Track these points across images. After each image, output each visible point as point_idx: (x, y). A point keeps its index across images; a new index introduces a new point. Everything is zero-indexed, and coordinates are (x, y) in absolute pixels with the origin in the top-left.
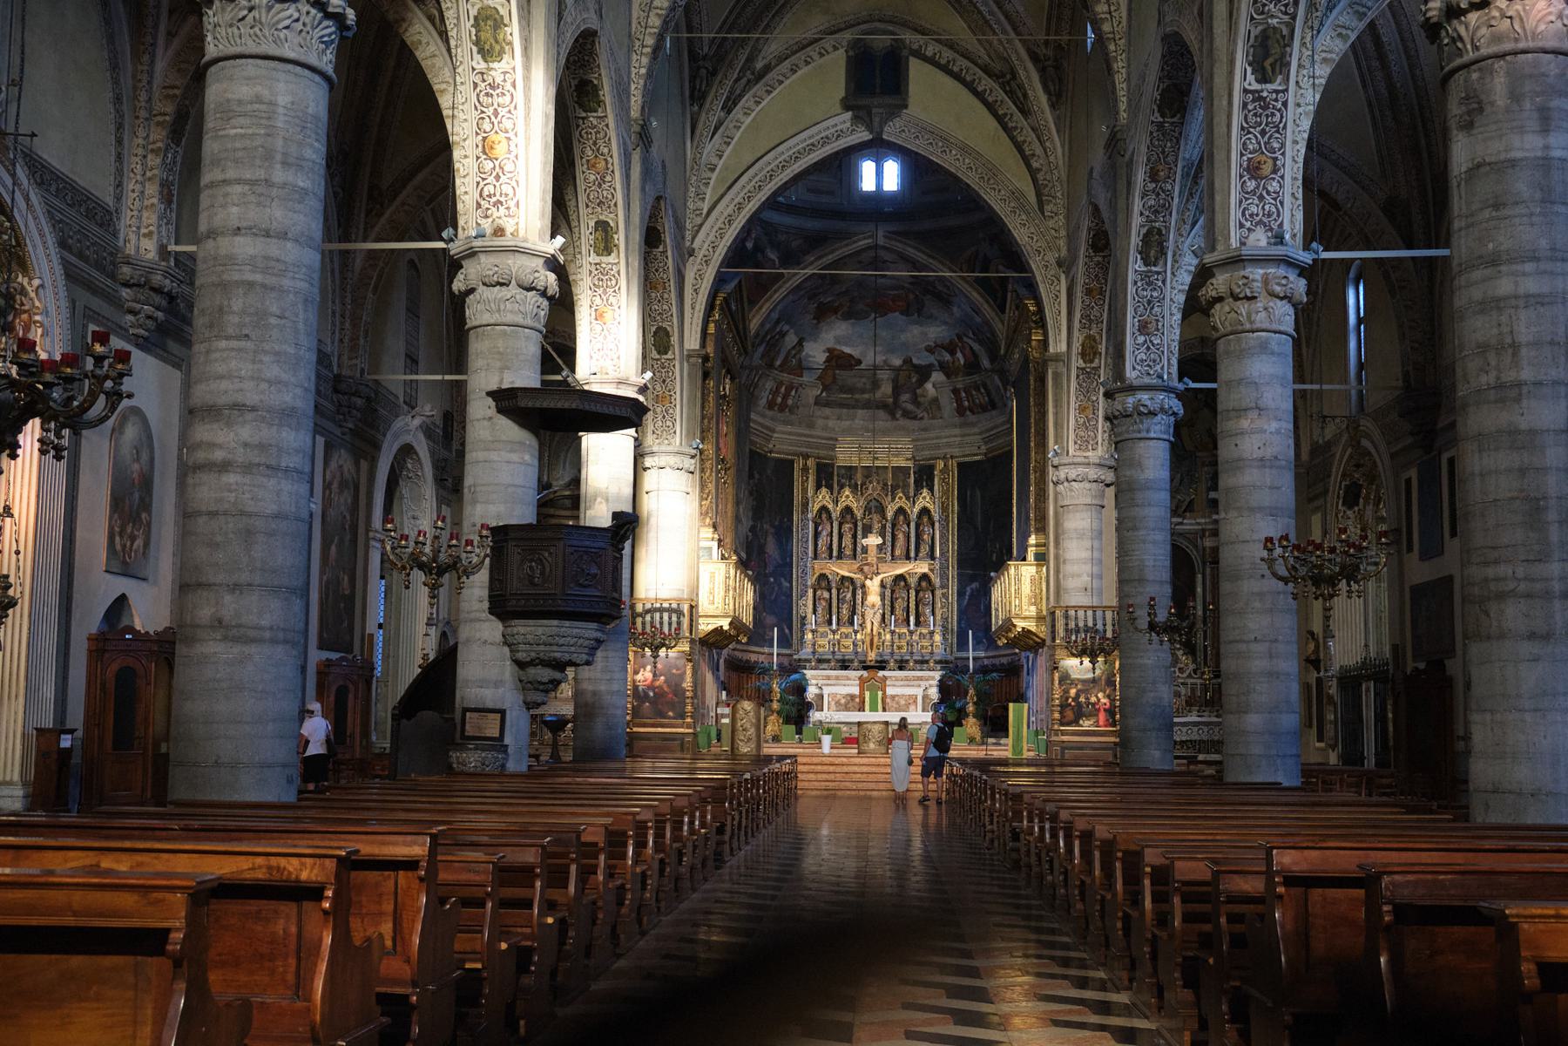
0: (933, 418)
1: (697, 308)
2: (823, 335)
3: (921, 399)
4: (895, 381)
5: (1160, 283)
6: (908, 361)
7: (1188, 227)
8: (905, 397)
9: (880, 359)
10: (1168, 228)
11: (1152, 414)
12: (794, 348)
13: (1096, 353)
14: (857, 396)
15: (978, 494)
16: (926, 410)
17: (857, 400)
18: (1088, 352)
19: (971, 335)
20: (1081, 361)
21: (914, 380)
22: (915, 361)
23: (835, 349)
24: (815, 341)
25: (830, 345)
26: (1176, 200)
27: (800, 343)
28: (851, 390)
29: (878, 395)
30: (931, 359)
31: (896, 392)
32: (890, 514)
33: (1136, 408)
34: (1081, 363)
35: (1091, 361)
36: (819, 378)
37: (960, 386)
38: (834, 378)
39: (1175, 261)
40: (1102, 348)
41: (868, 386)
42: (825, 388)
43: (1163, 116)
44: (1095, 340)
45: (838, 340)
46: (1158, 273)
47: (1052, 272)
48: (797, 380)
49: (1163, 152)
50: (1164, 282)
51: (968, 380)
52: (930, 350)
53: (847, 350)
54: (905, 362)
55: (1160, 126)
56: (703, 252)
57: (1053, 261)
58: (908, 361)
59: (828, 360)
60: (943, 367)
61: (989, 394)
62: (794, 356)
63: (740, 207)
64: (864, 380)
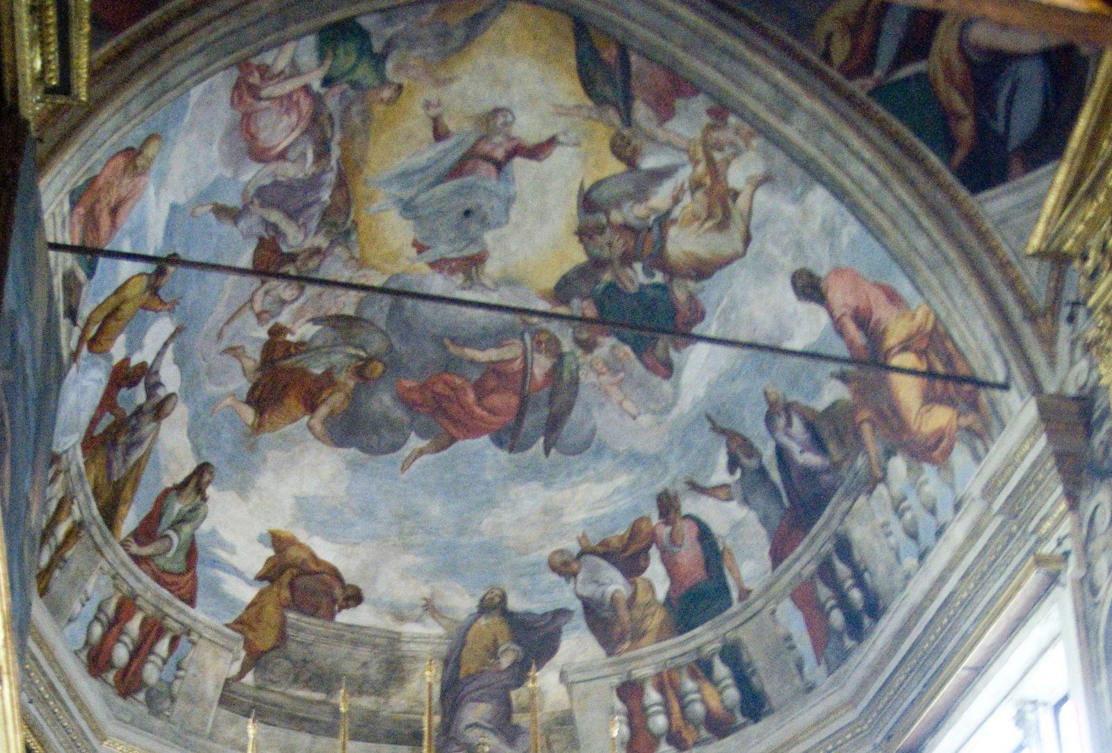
2: (265, 480)
4: (452, 662)
6: (493, 605)
8: (476, 712)
9: (410, 592)
12: (180, 488)
19: (720, 475)
21: (505, 662)
22: (515, 603)
23: (292, 542)
24: (243, 489)
25: (280, 525)
27: (199, 479)
28: (324, 680)
30: (565, 595)
36: (241, 624)
38: (282, 637)
41: (374, 672)
42: (255, 659)
45: (305, 508)
48: (175, 610)
51: (678, 648)
52: (564, 567)
53: (326, 551)
54: (485, 608)
58: (493, 605)
59: (270, 575)
62: (181, 521)
64: (364, 653)
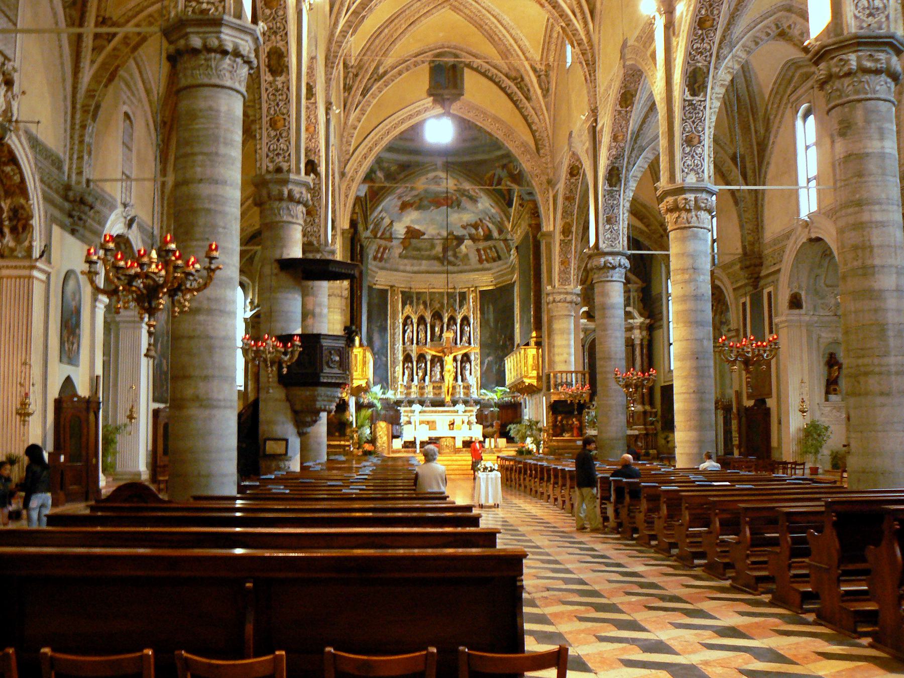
0: (466, 265)
1: (348, 205)
3: (458, 255)
5: (618, 196)
7: (631, 166)
10: (622, 167)
11: (614, 268)
13: (570, 232)
14: (423, 253)
15: (491, 307)
16: (461, 261)
17: (422, 255)
18: (566, 231)
20: (562, 236)
26: (626, 153)
29: (434, 252)
31: (445, 249)
32: (446, 320)
33: (605, 264)
34: (562, 237)
35: (568, 236)
37: (481, 247)
39: (625, 185)
40: (574, 229)
43: (622, 107)
44: (570, 225)
46: (617, 191)
47: (545, 187)
49: (621, 126)
50: (620, 196)
55: (620, 112)
56: (350, 175)
57: (545, 181)
60: (473, 238)
61: (497, 252)
63: (371, 150)
